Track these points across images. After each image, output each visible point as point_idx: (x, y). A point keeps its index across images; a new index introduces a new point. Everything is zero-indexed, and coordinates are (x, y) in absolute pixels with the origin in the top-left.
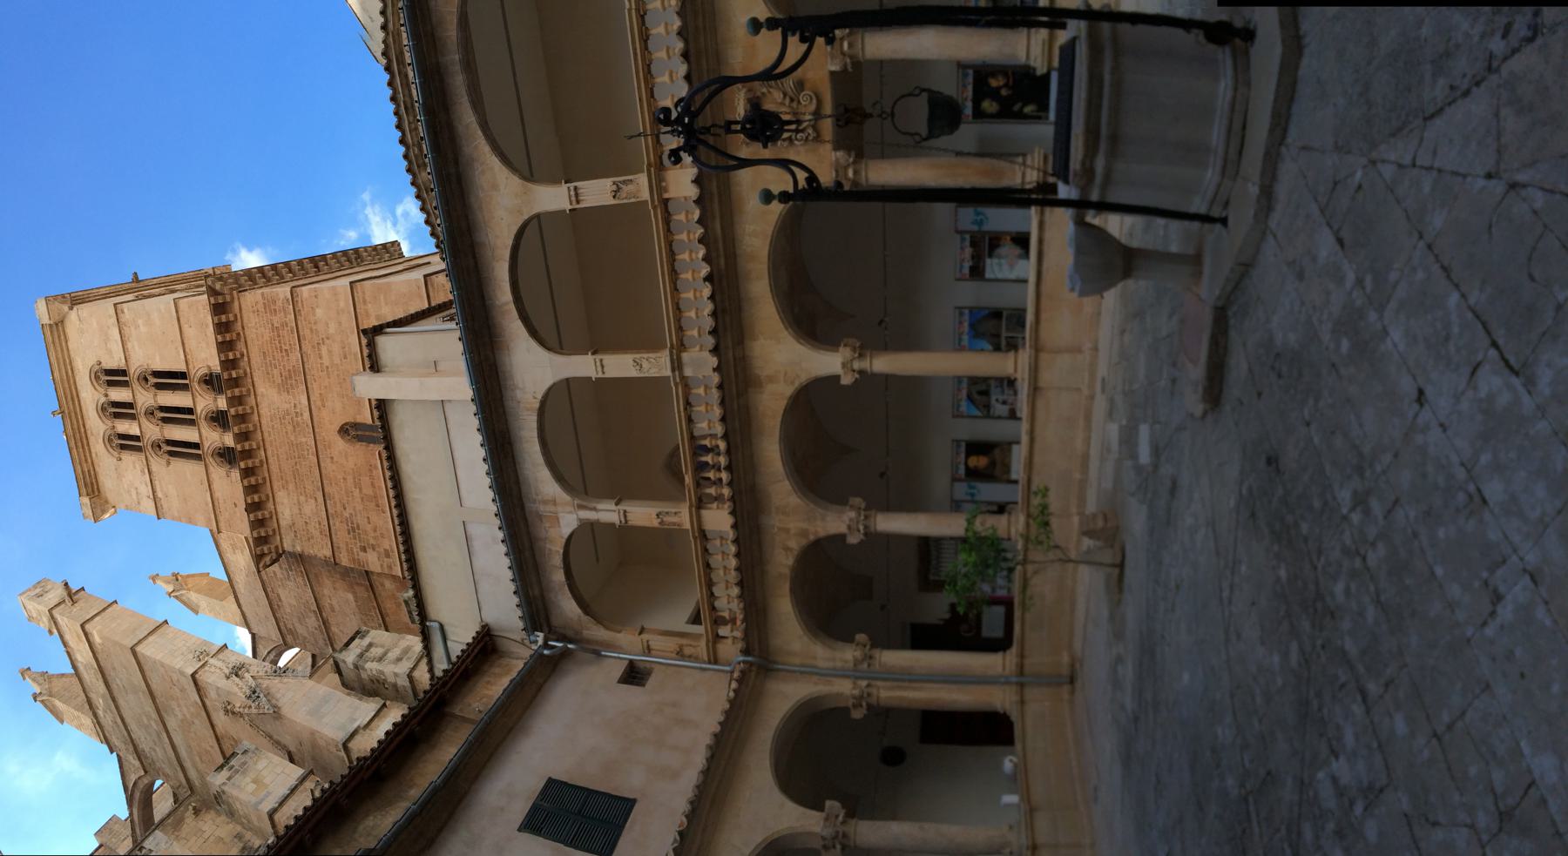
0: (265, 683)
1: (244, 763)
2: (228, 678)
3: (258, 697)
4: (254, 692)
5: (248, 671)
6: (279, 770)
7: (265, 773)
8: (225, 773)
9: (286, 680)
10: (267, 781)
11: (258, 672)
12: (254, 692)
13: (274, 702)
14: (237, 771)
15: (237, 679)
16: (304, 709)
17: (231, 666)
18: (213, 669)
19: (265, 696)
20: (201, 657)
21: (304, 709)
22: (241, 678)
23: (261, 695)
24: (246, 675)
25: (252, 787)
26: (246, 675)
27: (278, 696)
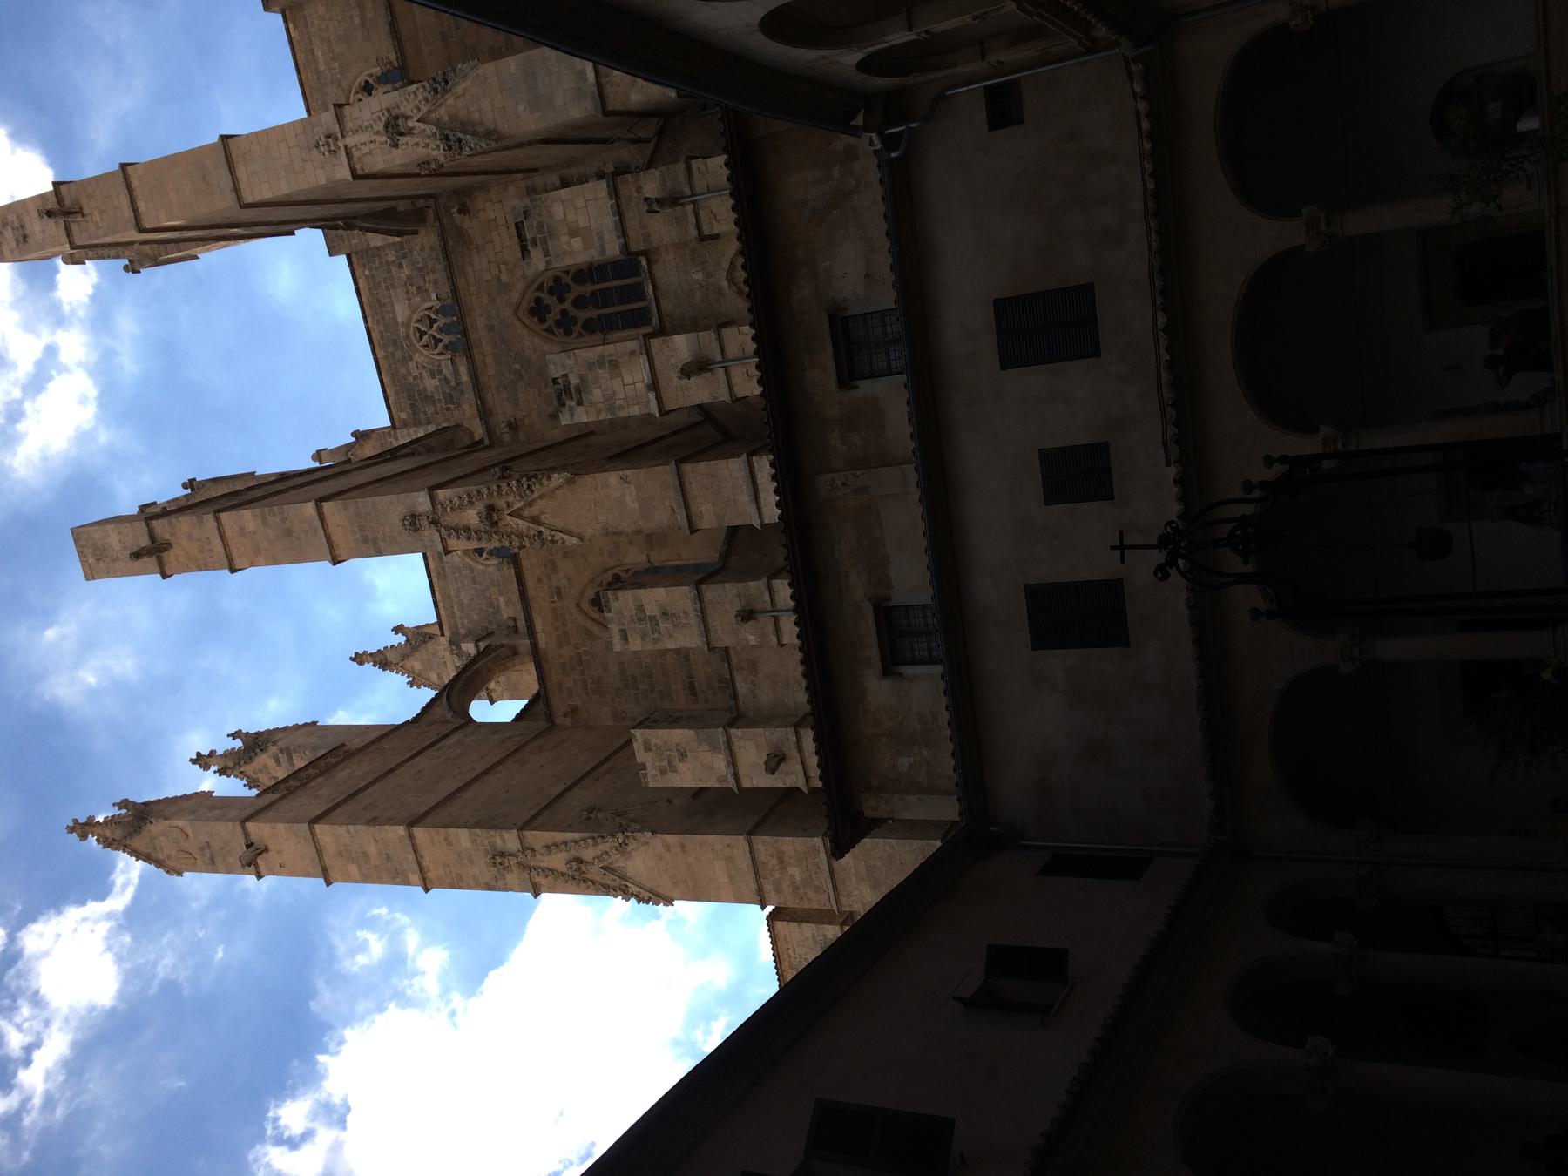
0: (443, 113)
1: (540, 226)
2: (396, 146)
3: (460, 140)
4: (447, 138)
5: (407, 118)
6: (580, 202)
7: (571, 218)
8: (536, 254)
9: (459, 89)
10: (583, 223)
11: (419, 109)
12: (447, 138)
13: (480, 129)
14: (544, 241)
15: (407, 139)
16: (521, 108)
17: (381, 127)
18: (365, 150)
19: (465, 133)
20: (333, 148)
21: (521, 108)
22: (410, 132)
23: (460, 135)
24: (410, 124)
25: (577, 243)
26: (410, 124)
27: (476, 116)
